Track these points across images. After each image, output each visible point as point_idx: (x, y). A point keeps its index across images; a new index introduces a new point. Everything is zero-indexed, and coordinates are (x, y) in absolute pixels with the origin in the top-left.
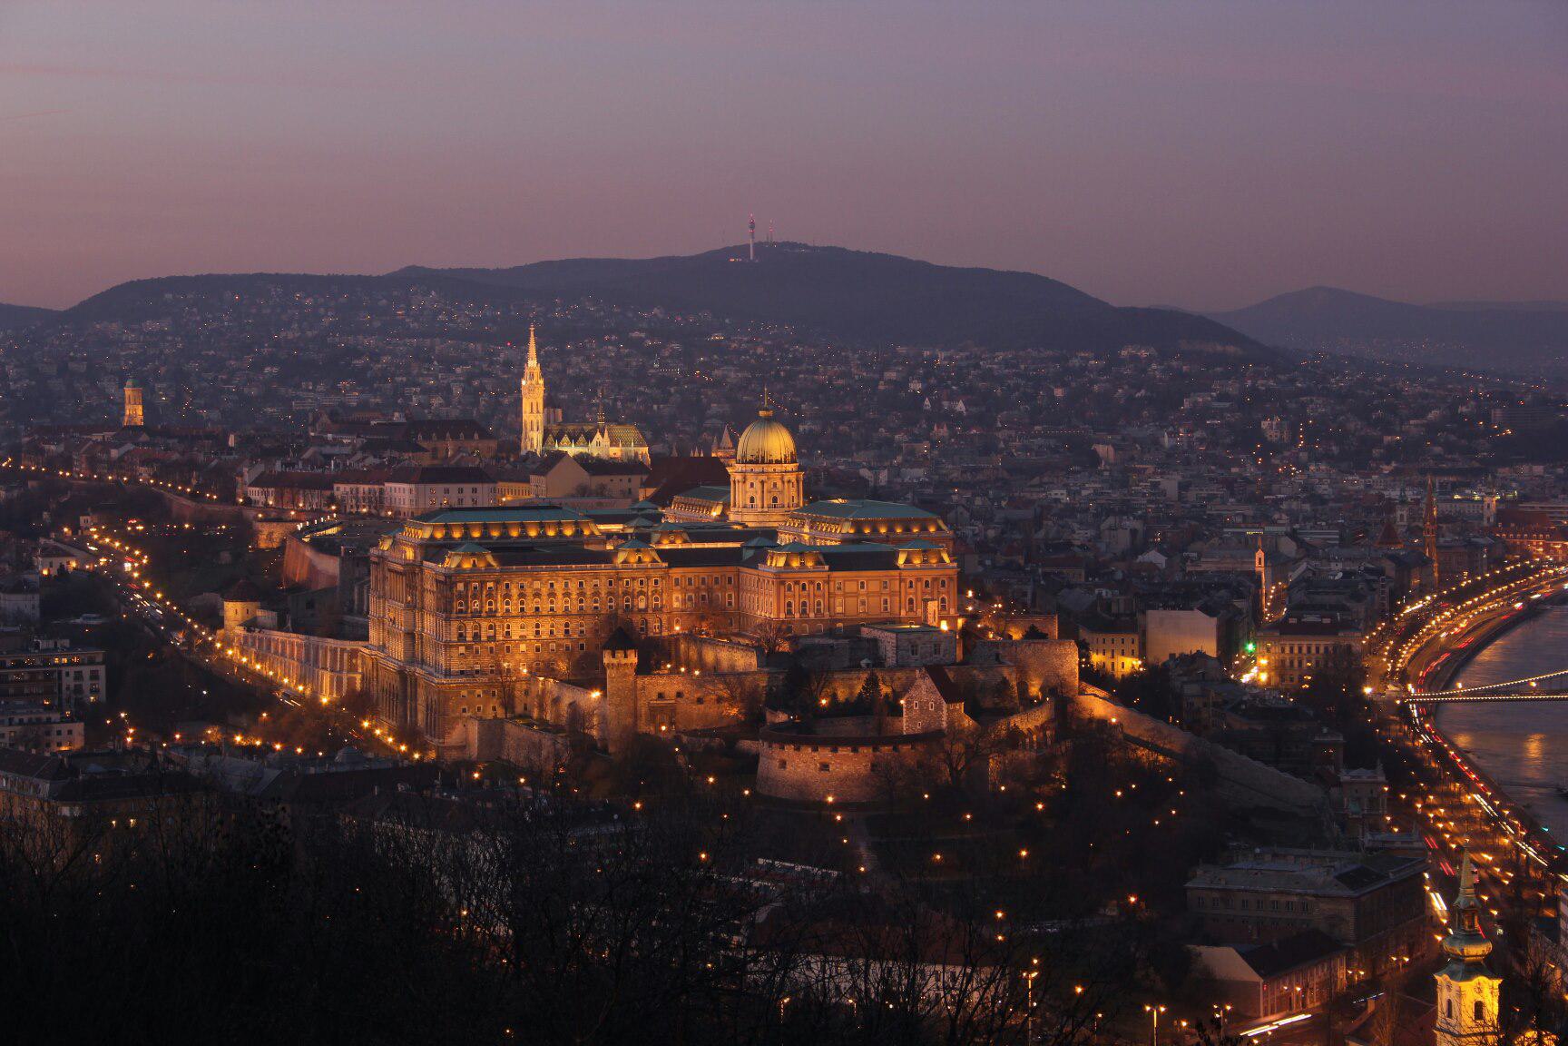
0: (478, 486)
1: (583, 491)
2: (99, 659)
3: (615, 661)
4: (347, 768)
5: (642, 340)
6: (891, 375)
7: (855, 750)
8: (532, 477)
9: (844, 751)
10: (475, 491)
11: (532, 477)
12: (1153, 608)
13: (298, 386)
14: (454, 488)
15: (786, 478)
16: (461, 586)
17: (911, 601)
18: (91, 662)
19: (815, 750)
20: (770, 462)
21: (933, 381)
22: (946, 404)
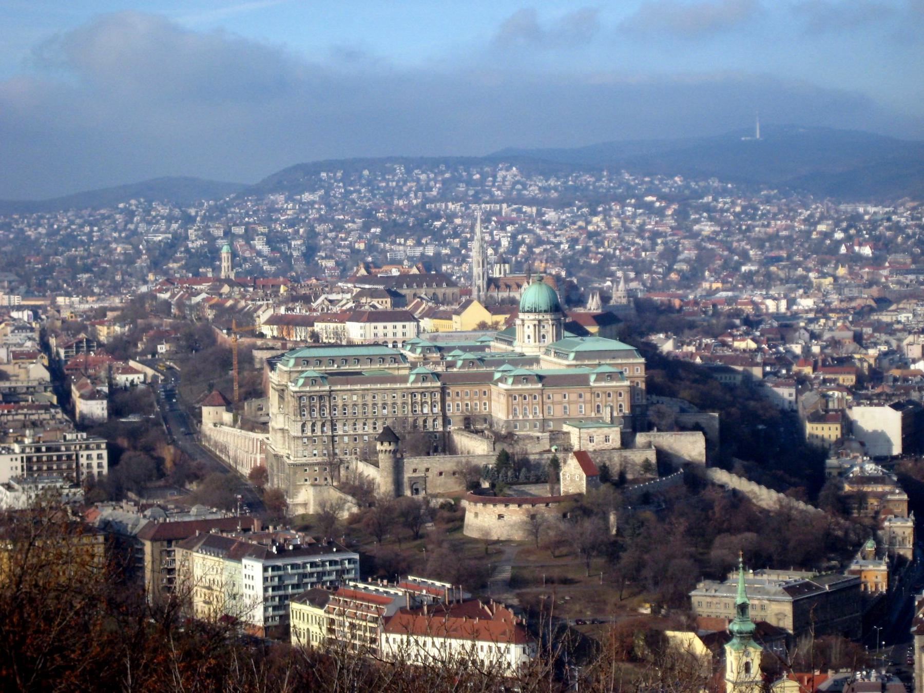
0: (407, 324)
1: (483, 326)
2: (103, 446)
4: (193, 519)
5: (653, 202)
6: (822, 227)
7: (519, 506)
8: (454, 317)
9: (513, 507)
10: (404, 327)
11: (454, 317)
12: (859, 404)
13: (393, 242)
14: (390, 325)
17: (598, 406)
18: (98, 447)
21: (852, 231)
22: (856, 248)
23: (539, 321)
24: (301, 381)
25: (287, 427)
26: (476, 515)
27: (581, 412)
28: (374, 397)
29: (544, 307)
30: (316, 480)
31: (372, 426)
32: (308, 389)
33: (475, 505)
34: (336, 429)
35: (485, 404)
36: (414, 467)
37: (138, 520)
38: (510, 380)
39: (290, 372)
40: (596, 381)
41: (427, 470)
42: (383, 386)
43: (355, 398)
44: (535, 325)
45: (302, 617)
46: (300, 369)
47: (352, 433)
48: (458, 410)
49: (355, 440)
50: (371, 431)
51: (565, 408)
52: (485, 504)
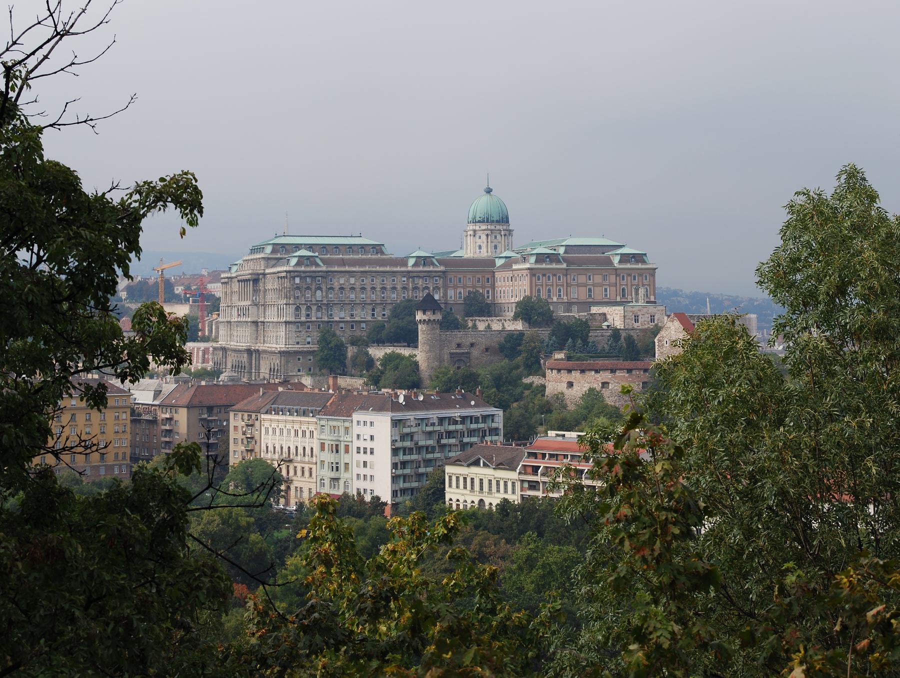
3: (425, 317)
15: (503, 233)
16: (297, 280)
17: (623, 289)
19: (597, 371)
20: (493, 221)
23: (491, 230)
24: (294, 261)
25: (262, 319)
26: (570, 385)
27: (606, 295)
28: (373, 281)
29: (495, 219)
30: (310, 370)
31: (370, 312)
32: (303, 269)
33: (569, 371)
34: (331, 315)
35: (488, 292)
36: (458, 341)
37: (160, 385)
38: (533, 259)
39: (269, 259)
40: (620, 262)
41: (472, 345)
42: (382, 269)
43: (352, 281)
44: (487, 235)
45: (468, 483)
46: (279, 256)
47: (348, 319)
48: (460, 297)
49: (352, 327)
50: (369, 318)
51: (590, 290)
52: (583, 371)
